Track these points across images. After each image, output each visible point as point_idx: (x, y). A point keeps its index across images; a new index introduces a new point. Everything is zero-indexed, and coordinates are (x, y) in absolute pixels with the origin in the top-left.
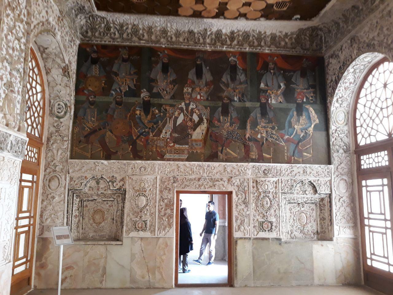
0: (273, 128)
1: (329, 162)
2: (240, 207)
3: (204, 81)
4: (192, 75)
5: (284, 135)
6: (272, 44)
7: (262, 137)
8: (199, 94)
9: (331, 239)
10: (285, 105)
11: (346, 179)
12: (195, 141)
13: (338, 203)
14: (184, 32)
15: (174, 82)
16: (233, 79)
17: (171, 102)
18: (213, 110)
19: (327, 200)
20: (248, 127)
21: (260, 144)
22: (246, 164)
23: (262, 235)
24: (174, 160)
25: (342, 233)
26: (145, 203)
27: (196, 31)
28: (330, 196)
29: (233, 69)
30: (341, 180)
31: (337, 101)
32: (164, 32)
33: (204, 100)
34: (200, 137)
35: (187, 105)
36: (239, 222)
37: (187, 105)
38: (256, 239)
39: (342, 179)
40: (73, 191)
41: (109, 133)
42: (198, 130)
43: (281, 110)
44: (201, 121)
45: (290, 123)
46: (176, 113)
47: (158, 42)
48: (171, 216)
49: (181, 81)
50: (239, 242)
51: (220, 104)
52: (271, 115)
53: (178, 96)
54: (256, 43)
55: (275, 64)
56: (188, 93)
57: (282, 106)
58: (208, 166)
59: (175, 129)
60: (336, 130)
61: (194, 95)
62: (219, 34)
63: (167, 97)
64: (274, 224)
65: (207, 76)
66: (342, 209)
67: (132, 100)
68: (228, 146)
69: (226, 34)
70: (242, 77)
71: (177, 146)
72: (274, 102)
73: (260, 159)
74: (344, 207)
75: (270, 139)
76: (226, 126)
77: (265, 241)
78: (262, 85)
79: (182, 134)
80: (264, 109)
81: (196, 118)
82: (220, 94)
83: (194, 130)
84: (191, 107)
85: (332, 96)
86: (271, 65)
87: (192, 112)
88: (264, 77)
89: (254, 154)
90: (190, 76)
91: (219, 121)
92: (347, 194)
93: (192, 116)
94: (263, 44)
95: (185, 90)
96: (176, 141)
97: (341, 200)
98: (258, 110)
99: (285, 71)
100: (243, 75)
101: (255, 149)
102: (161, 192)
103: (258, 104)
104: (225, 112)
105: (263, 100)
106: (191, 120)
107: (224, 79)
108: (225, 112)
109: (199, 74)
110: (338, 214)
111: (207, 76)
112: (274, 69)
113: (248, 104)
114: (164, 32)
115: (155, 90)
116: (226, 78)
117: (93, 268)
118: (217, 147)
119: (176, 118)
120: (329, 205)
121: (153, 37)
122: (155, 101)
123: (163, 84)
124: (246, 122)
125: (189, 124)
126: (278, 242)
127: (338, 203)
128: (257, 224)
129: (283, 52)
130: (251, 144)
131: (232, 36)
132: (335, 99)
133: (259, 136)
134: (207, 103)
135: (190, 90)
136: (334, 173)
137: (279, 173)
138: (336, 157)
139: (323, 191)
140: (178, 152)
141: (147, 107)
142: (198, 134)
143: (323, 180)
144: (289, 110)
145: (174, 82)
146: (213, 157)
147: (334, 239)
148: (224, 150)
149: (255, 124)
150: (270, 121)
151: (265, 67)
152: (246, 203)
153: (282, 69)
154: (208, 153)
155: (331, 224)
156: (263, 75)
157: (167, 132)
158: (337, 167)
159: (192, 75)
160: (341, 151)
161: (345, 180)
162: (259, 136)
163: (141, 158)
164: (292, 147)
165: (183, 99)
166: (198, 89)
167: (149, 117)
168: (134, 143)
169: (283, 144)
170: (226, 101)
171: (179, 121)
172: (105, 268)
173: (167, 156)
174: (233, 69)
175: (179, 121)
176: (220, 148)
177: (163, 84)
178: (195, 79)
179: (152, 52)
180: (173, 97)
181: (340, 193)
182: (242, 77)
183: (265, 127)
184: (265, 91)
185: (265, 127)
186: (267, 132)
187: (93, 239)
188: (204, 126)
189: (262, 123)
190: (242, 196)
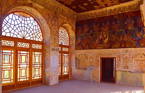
0: (130, 37)
2: (118, 62)
3: (107, 25)
4: (104, 24)
5: (134, 39)
6: (129, 9)
7: (126, 40)
8: (106, 29)
10: (134, 29)
12: (105, 43)
14: (101, 12)
15: (99, 27)
16: (116, 23)
17: (98, 33)
18: (110, 34)
20: (121, 37)
21: (125, 43)
22: (120, 49)
23: (125, 70)
24: (99, 49)
26: (92, 60)
27: (104, 11)
29: (116, 20)
32: (95, 13)
33: (107, 31)
34: (106, 42)
35: (103, 33)
36: (117, 66)
37: (103, 33)
38: (123, 71)
40: (76, 58)
41: (83, 43)
42: (106, 40)
43: (132, 30)
44: (107, 37)
45: (136, 34)
46: (100, 36)
47: (94, 16)
48: (99, 64)
49: (101, 27)
50: (117, 72)
51: (112, 31)
52: (129, 32)
53: (100, 31)
54: (123, 10)
55: (130, 15)
56: (103, 30)
57: (133, 29)
58: (109, 50)
59: (99, 40)
61: (104, 30)
62: (111, 10)
63: (97, 31)
64: (129, 67)
65: (108, 23)
67: (88, 34)
68: (115, 44)
69: (113, 10)
70: (119, 22)
71: (100, 45)
72: (130, 28)
73: (125, 47)
75: (128, 41)
76: (114, 37)
77: (126, 72)
78: (126, 23)
79: (101, 41)
80: (126, 31)
81: (105, 36)
82: (112, 28)
83: (105, 40)
84: (104, 33)
86: (129, 16)
87: (104, 34)
88: (126, 20)
89: (123, 46)
90: (103, 25)
91: (112, 36)
93: (104, 36)
94: (126, 9)
95: (102, 29)
96: (100, 44)
98: (125, 32)
99: (134, 17)
100: (119, 21)
101: (123, 44)
102: (96, 58)
103: (124, 30)
104: (114, 33)
105: (126, 28)
106: (104, 37)
107: (113, 24)
108: (114, 33)
109: (106, 24)
111: (108, 23)
112: (130, 17)
113: (120, 30)
114: (95, 13)
115: (94, 30)
116: (114, 23)
117: (81, 75)
118: (111, 44)
119: (100, 37)
121: (93, 16)
122: (94, 33)
123: (96, 28)
124: (120, 36)
125: (103, 38)
126: (130, 72)
128: (123, 67)
129: (133, 11)
130: (122, 42)
131: (115, 10)
133: (125, 40)
134: (108, 32)
135: (103, 28)
137: (131, 51)
140: (101, 46)
141: (92, 35)
142: (106, 41)
144: (136, 30)
145: (99, 27)
146: (110, 47)
148: (114, 45)
149: (123, 36)
150: (129, 35)
151: (127, 17)
152: (120, 60)
153: (132, 17)
154: (109, 46)
156: (126, 20)
157: (97, 41)
159: (104, 24)
162: (125, 40)
163: (91, 49)
164: (136, 42)
165: (101, 31)
166: (105, 28)
167: (93, 38)
168: (89, 45)
169: (133, 41)
170: (114, 30)
171: (100, 38)
172: (83, 76)
173: (97, 48)
174: (116, 20)
175: (100, 38)
176: (112, 45)
177: (96, 28)
178: (104, 25)
179: (93, 20)
180: (99, 31)
182: (119, 22)
183: (127, 37)
184: (126, 25)
185: (127, 37)
186: (127, 38)
187: (82, 69)
188: (107, 39)
189: (126, 36)
190: (119, 59)
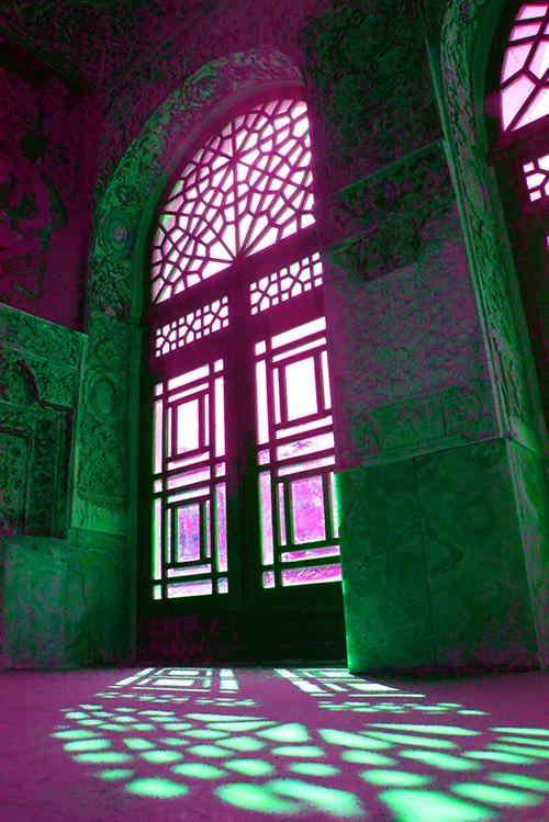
1: (80, 324)
9: (62, 535)
11: (116, 382)
13: (87, 436)
19: (61, 425)
25: (91, 518)
28: (70, 412)
30: (101, 380)
31: (118, 191)
39: (107, 379)
60: (105, 259)
66: (97, 454)
74: (101, 453)
85: (108, 176)
92: (111, 420)
97: (98, 430)
110: (86, 467)
120: (64, 439)
127: (87, 436)
132: (114, 184)
136: (87, 360)
138: (102, 319)
139: (58, 397)
143: (56, 369)
147: (70, 534)
155: (65, 490)
158: (97, 346)
160: (110, 311)
161: (112, 383)
181: (95, 408)
